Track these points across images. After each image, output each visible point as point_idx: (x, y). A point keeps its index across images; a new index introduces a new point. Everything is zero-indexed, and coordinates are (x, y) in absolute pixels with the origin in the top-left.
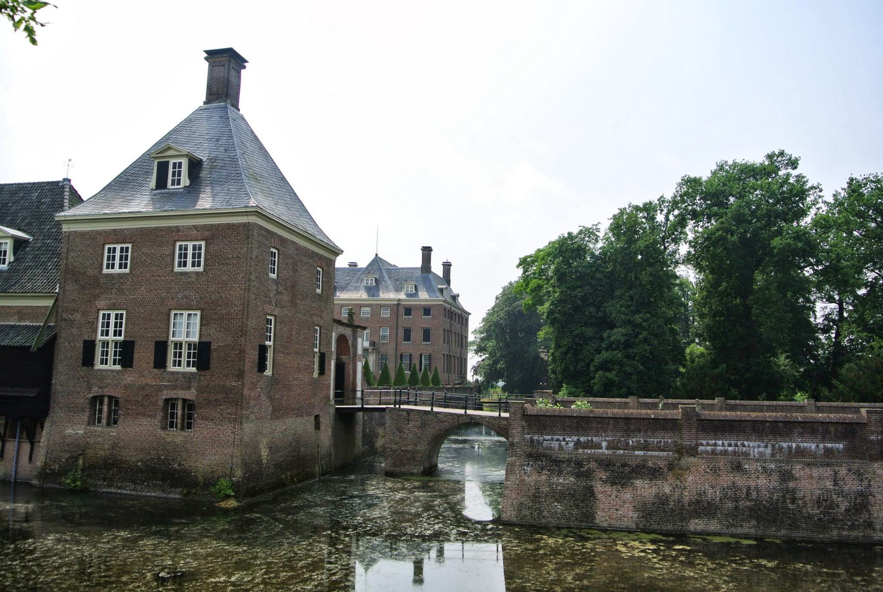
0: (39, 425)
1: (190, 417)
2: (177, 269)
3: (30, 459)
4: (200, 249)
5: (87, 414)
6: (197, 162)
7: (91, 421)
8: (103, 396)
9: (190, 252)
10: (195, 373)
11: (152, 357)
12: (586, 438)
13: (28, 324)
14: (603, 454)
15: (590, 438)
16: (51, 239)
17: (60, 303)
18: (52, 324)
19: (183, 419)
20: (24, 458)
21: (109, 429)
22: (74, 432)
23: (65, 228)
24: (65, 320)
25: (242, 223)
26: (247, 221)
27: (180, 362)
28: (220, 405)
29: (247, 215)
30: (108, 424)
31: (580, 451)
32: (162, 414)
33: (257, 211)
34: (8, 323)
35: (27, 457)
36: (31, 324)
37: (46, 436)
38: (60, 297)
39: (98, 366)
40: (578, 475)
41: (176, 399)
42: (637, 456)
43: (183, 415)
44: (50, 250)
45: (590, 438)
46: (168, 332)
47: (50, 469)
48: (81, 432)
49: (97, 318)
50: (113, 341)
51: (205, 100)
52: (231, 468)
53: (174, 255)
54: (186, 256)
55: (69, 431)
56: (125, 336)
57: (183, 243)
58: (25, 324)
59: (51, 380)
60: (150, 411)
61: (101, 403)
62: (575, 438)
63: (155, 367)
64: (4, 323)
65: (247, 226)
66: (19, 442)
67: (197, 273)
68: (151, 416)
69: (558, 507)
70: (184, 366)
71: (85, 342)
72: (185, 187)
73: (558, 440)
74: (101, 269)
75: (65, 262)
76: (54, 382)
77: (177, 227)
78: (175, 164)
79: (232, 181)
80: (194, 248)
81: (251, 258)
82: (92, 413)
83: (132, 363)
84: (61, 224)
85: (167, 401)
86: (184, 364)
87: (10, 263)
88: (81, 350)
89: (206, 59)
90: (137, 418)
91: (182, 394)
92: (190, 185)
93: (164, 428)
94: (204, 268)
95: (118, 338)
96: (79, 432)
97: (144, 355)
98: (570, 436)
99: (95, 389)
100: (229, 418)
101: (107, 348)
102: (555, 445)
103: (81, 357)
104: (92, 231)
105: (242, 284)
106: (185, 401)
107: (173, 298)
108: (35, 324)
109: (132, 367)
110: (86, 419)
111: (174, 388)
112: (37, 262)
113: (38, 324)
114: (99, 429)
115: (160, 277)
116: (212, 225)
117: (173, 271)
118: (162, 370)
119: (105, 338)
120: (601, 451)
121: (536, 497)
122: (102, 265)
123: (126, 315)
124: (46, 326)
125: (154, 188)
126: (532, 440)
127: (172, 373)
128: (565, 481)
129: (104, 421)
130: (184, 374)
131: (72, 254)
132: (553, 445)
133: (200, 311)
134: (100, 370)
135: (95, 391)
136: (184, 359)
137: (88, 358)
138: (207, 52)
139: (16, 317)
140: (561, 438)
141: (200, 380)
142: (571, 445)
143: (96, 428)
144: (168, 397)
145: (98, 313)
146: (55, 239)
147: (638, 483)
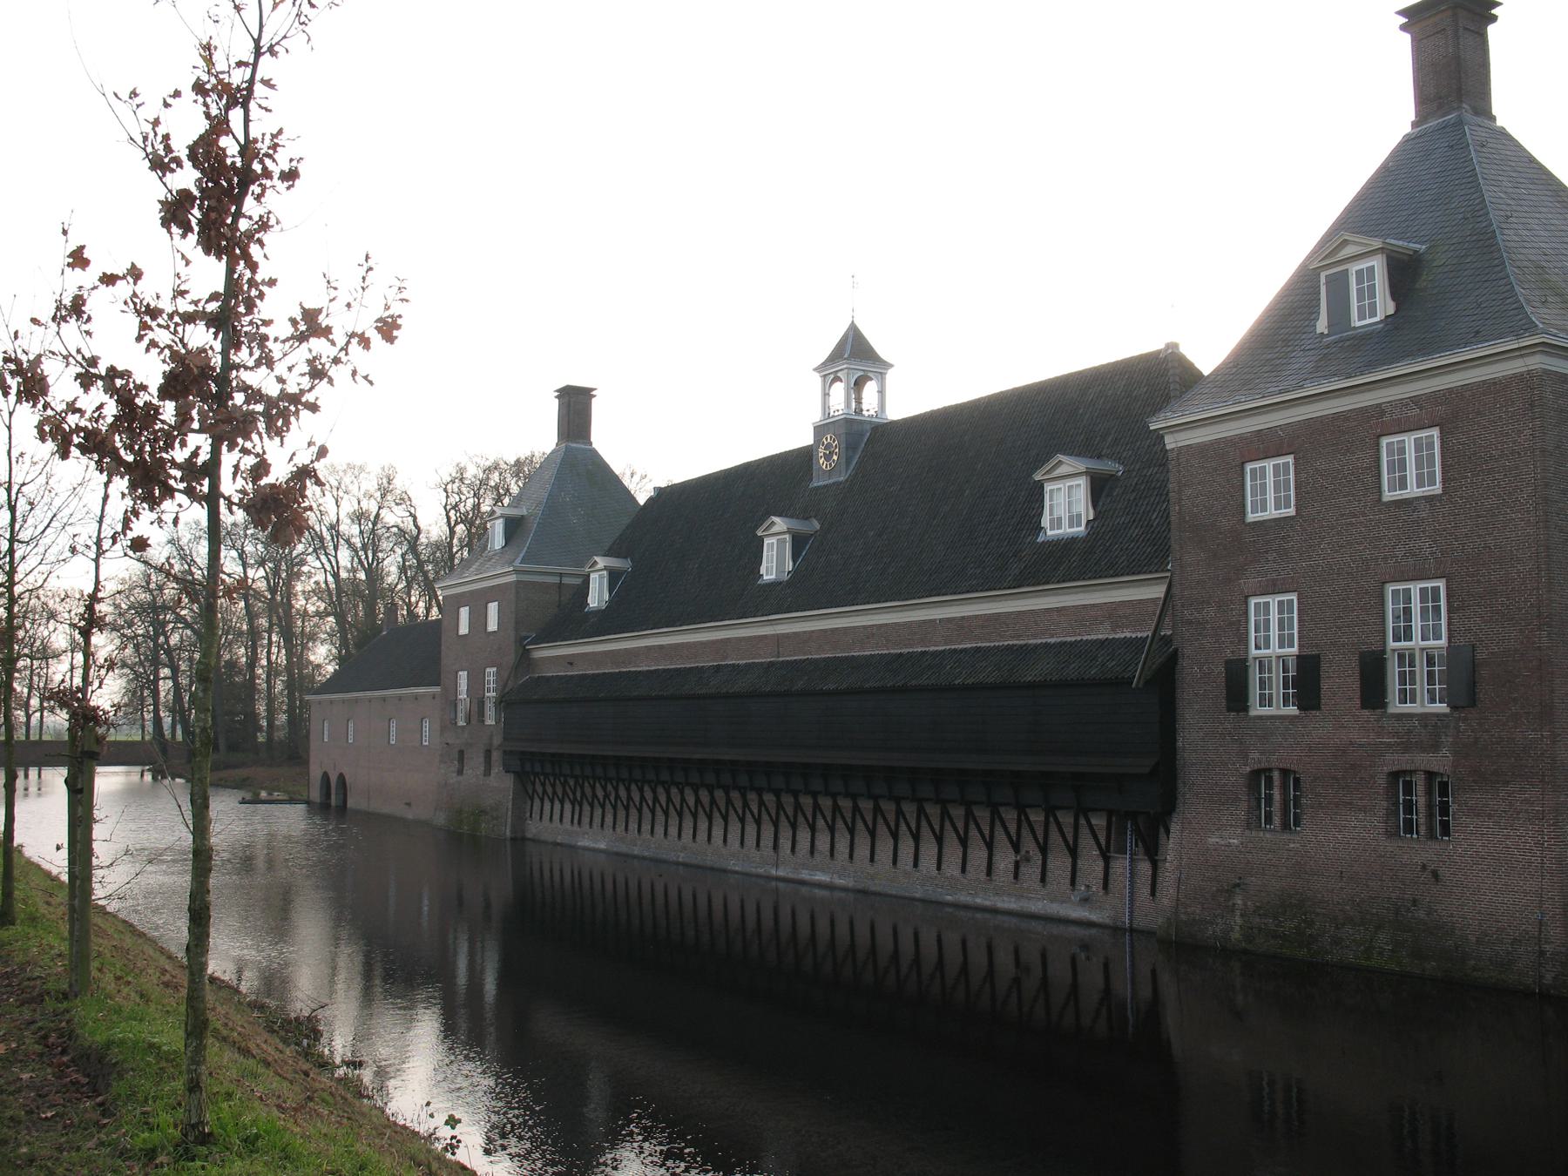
0: (1162, 830)
1: (1445, 810)
2: (1388, 496)
3: (1153, 893)
4: (1431, 446)
5: (1244, 806)
6: (1405, 258)
7: (1252, 823)
8: (1270, 770)
9: (1411, 456)
10: (1445, 715)
11: (1357, 686)
13: (1128, 635)
16: (1155, 466)
17: (1176, 590)
18: (1169, 633)
19: (1430, 816)
20: (1145, 891)
21: (1286, 836)
22: (1223, 843)
23: (1171, 442)
24: (1190, 622)
25: (1515, 376)
27: (1413, 692)
28: (1508, 783)
29: (1522, 356)
30: (1285, 826)
32: (1385, 804)
33: (1543, 342)
34: (1094, 637)
35: (1146, 891)
36: (1134, 636)
37: (1172, 848)
38: (1176, 578)
39: (1257, 710)
41: (1411, 772)
43: (1430, 806)
44: (1154, 488)
46: (1384, 632)
47: (1185, 913)
48: (1235, 841)
49: (1246, 613)
50: (1279, 657)
51: (1413, 118)
52: (1541, 923)
53: (1378, 467)
54: (1403, 466)
55: (1213, 840)
56: (1300, 646)
57: (1395, 439)
58: (1123, 636)
59: (1175, 741)
60: (1361, 799)
61: (1269, 785)
63: (1364, 706)
64: (1089, 638)
65: (1524, 380)
66: (1132, 860)
67: (1430, 499)
68: (1364, 809)
70: (1422, 701)
71: (1228, 663)
72: (1387, 317)
74: (1243, 513)
75: (1177, 508)
76: (1180, 744)
77: (1379, 405)
78: (1359, 273)
79: (1486, 284)
80: (1418, 448)
81: (1543, 451)
82: (1254, 803)
83: (1319, 697)
84: (1163, 437)
85: (1395, 776)
86: (1422, 695)
87: (1088, 522)
88: (1222, 679)
89: (1404, 28)
90: (1336, 814)
91: (1424, 761)
92: (1396, 312)
93: (1392, 834)
94: (1444, 488)
95: (1287, 651)
96: (1231, 841)
97: (1340, 682)
99: (1254, 755)
100: (1526, 811)
101: (1270, 671)
103: (1224, 695)
104: (1218, 441)
105: (1528, 512)
106: (1430, 775)
107: (1385, 558)
108: (1139, 635)
109: (1318, 708)
110: (1241, 812)
111: (1406, 747)
112: (1133, 514)
113: (1145, 635)
114: (1268, 835)
115: (1355, 516)
116: (1450, 390)
117: (1380, 500)
118: (1379, 711)
119: (1263, 652)
122: (1243, 506)
123: (1299, 603)
124: (1156, 639)
125: (1326, 332)
127: (1400, 717)
129: (1277, 820)
130: (1424, 717)
131: (1188, 492)
133: (1444, 580)
134: (1260, 718)
135: (1256, 759)
136: (1421, 685)
137: (1237, 696)
138: (1402, 13)
139: (1107, 625)
143: (1261, 834)
144: (1395, 769)
145: (1246, 603)
146: (1160, 465)
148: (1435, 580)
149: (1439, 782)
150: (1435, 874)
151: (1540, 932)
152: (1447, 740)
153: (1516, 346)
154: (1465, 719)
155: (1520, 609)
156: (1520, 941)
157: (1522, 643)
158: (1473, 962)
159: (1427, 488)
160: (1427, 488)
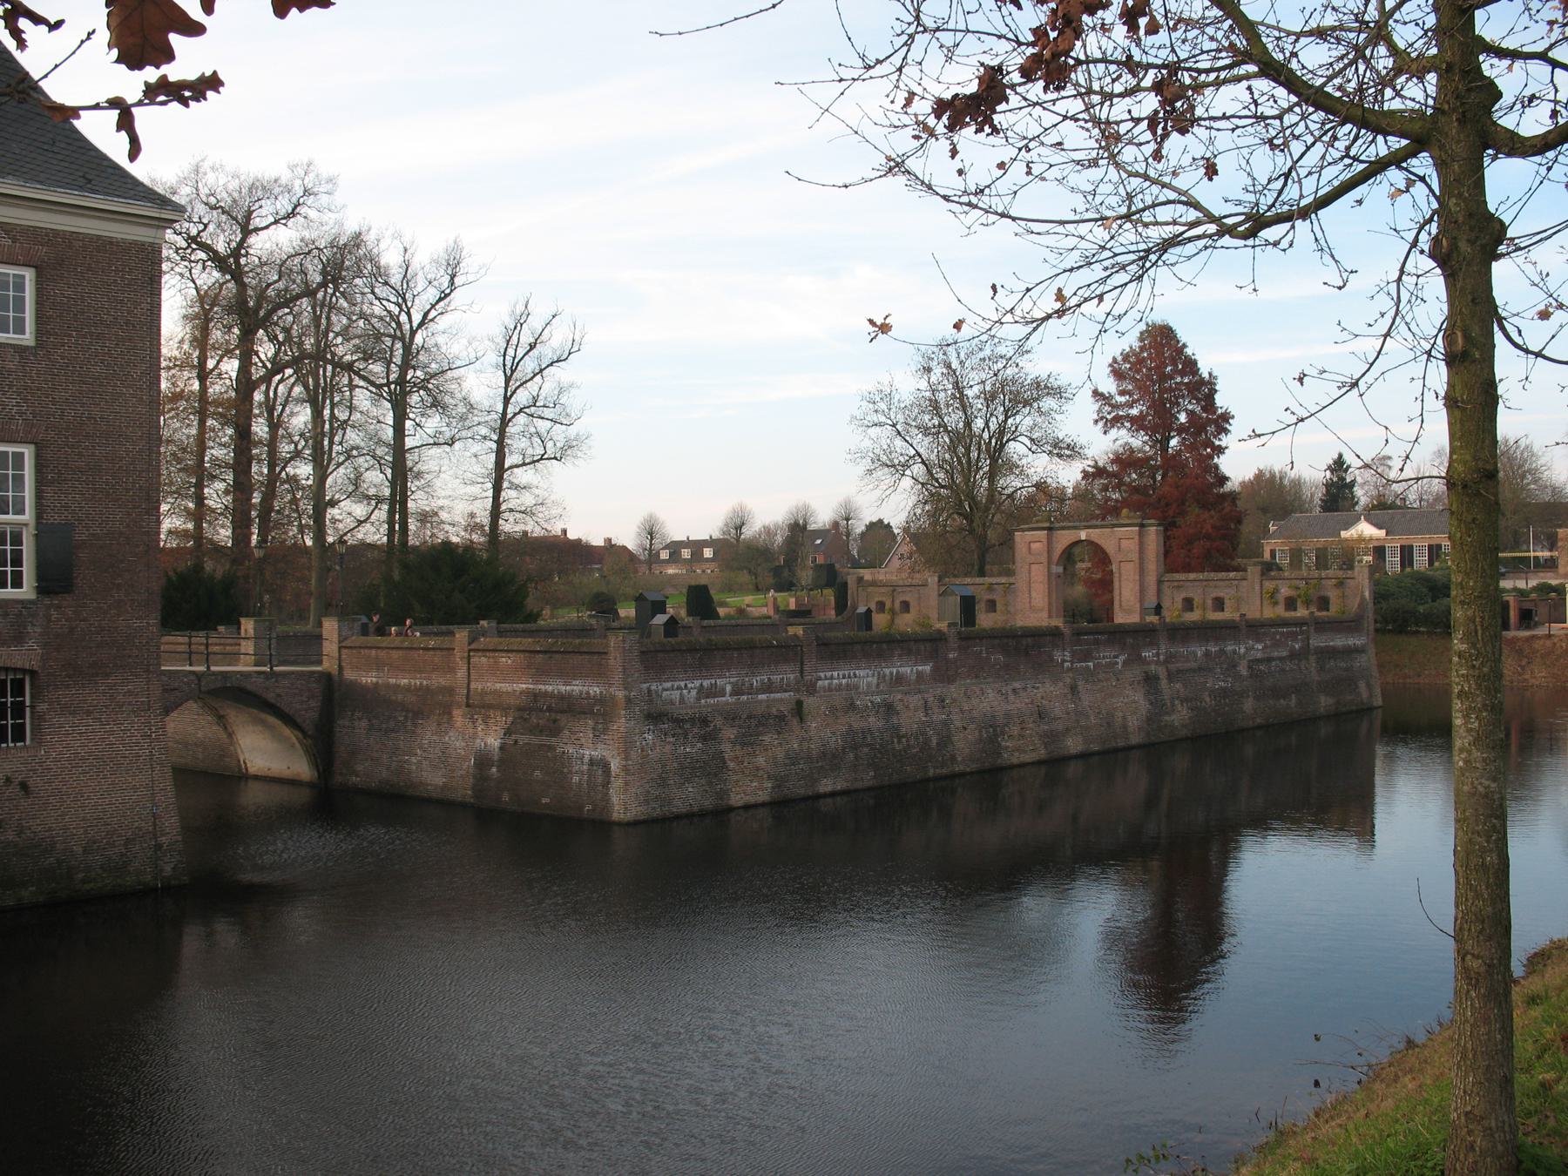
10: (30, 602)
12: (709, 682)
14: (727, 703)
15: (713, 681)
25: (135, 243)
26: (151, 240)
28: (107, 675)
31: (703, 701)
40: (704, 738)
42: (761, 701)
45: (713, 681)
62: (697, 683)
69: (690, 789)
73: (679, 688)
98: (692, 679)
102: (676, 695)
105: (141, 389)
120: (724, 699)
121: (662, 782)
126: (649, 691)
128: (693, 748)
132: (673, 697)
140: (682, 684)
141: (48, 618)
142: (694, 693)
147: (767, 738)
148: (20, 445)
149: (11, 680)
150: (24, 786)
151: (155, 824)
152: (34, 630)
153: (157, 215)
154: (58, 607)
155: (128, 490)
156: (134, 839)
157: (128, 526)
158: (80, 876)
159: (11, 335)
160: (11, 335)
